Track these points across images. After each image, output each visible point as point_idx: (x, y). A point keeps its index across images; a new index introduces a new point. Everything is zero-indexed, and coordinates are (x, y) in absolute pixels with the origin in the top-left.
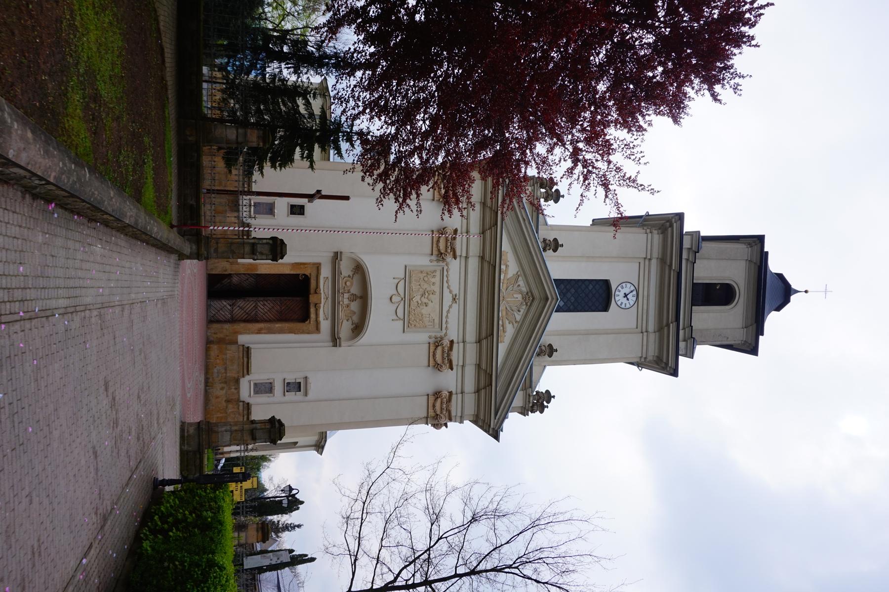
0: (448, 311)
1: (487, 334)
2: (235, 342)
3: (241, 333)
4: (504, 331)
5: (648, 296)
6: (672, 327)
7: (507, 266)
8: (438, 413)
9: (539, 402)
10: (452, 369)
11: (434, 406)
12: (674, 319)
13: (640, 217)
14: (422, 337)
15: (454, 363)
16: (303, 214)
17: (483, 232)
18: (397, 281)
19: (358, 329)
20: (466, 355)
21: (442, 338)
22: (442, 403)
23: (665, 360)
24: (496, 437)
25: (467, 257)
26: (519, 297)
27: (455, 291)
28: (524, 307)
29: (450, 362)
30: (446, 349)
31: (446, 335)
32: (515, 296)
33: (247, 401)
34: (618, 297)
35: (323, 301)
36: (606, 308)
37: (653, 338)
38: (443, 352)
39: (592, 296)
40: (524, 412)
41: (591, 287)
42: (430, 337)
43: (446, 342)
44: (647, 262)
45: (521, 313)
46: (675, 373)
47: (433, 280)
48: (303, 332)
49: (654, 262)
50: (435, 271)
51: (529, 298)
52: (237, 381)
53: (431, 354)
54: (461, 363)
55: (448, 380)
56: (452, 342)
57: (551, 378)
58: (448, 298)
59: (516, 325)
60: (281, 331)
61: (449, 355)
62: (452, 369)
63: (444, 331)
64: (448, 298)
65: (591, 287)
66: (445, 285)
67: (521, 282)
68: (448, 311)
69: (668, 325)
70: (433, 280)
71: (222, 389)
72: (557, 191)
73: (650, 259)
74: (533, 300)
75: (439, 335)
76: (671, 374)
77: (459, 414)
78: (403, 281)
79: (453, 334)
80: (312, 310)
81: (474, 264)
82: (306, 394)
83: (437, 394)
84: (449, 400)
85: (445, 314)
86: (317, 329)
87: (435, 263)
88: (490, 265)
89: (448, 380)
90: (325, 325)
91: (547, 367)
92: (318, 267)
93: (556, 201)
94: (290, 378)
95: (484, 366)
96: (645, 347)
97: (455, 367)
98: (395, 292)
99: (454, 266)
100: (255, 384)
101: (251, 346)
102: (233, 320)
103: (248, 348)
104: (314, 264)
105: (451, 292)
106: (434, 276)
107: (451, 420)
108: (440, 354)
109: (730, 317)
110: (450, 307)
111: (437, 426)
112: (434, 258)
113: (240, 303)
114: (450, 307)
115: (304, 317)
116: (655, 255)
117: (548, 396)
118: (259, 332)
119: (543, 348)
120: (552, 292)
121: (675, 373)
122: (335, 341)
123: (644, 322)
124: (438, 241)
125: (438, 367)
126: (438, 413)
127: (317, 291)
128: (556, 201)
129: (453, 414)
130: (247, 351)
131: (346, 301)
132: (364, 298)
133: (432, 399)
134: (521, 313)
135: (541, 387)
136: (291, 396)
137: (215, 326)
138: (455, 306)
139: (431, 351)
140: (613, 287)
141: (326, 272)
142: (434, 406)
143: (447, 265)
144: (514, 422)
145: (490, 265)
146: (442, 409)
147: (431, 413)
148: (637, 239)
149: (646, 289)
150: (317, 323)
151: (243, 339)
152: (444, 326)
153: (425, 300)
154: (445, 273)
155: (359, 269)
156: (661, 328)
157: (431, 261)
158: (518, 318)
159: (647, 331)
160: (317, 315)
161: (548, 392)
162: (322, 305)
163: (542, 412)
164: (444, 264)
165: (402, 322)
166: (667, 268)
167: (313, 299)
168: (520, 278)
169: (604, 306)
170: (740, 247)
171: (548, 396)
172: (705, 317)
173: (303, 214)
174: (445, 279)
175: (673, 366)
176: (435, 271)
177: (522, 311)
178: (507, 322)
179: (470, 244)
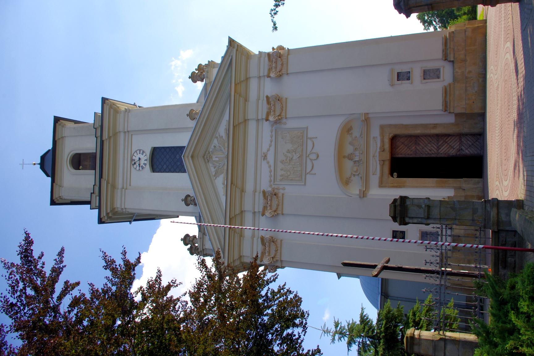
1: (238, 127)
2: (457, 115)
3: (452, 124)
5: (124, 160)
6: (105, 136)
8: (279, 58)
10: (267, 97)
11: (282, 65)
12: (105, 143)
13: (135, 220)
14: (291, 124)
16: (394, 231)
17: (242, 212)
18: (313, 172)
19: (347, 129)
20: (255, 108)
23: (112, 110)
24: (231, 42)
25: (255, 191)
26: (214, 159)
27: (264, 164)
28: (211, 150)
29: (268, 102)
31: (272, 126)
32: (217, 159)
33: (446, 62)
34: (145, 158)
35: (377, 154)
37: (120, 128)
38: (274, 111)
39: (165, 160)
40: (211, 64)
41: (165, 167)
43: (271, 118)
45: (213, 145)
46: (104, 100)
47: (283, 172)
48: (395, 126)
49: (120, 186)
50: (281, 180)
51: (207, 157)
52: (455, 79)
53: (284, 109)
58: (271, 157)
59: (217, 135)
60: (415, 126)
61: (270, 109)
62: (267, 97)
63: (273, 128)
64: (271, 157)
65: (165, 167)
66: (272, 168)
67: (213, 170)
69: (109, 137)
70: (283, 172)
71: (470, 72)
72: (186, 244)
73: (123, 188)
74: (204, 157)
76: (107, 99)
78: (308, 171)
79: (266, 127)
80: (387, 146)
81: (249, 186)
82: (392, 71)
83: (280, 76)
85: (273, 143)
86: (382, 127)
87: (281, 187)
88: (235, 185)
90: (375, 132)
92: (381, 185)
93: (187, 236)
94: (405, 85)
95: (242, 100)
96: (126, 119)
98: (314, 162)
99: (265, 185)
100: (438, 77)
101: (443, 113)
102: (460, 135)
103: (446, 111)
104: (385, 187)
105: (268, 163)
106: (281, 176)
107: (269, 54)
108: (276, 107)
109: (74, 145)
110: (268, 150)
111: (281, 48)
112: (281, 191)
113: (453, 152)
114: (268, 150)
115: (394, 139)
116: (119, 191)
117: (194, 78)
118: (435, 126)
120: (188, 163)
121: (104, 100)
122: (367, 120)
123: (126, 140)
124: (278, 205)
125: (279, 99)
127: (383, 162)
128: (187, 236)
129: (267, 58)
130: (446, 107)
131: (357, 153)
132: (341, 156)
133: (284, 71)
134: (213, 145)
135: (200, 85)
136: (404, 69)
137: (476, 130)
138: (265, 150)
139: (284, 111)
140: (148, 167)
141: (375, 179)
142: (282, 65)
143: (271, 186)
145: (235, 185)
146: (276, 63)
148: (130, 203)
149: (126, 165)
150: (382, 134)
151: (451, 119)
152: (274, 133)
153: (289, 155)
154: (272, 179)
155: (346, 182)
156: (116, 134)
157: (284, 189)
158: (215, 142)
160: (382, 141)
161: (195, 81)
162: (378, 150)
164: (273, 186)
165: (309, 136)
166: (110, 182)
167: (387, 156)
168: (214, 174)
169: (155, 151)
170: (67, 195)
171: (194, 78)
172: (88, 145)
173: (394, 231)
174: (272, 173)
175: (105, 106)
176: (281, 180)
177: (212, 147)
178: (224, 137)
179: (252, 202)
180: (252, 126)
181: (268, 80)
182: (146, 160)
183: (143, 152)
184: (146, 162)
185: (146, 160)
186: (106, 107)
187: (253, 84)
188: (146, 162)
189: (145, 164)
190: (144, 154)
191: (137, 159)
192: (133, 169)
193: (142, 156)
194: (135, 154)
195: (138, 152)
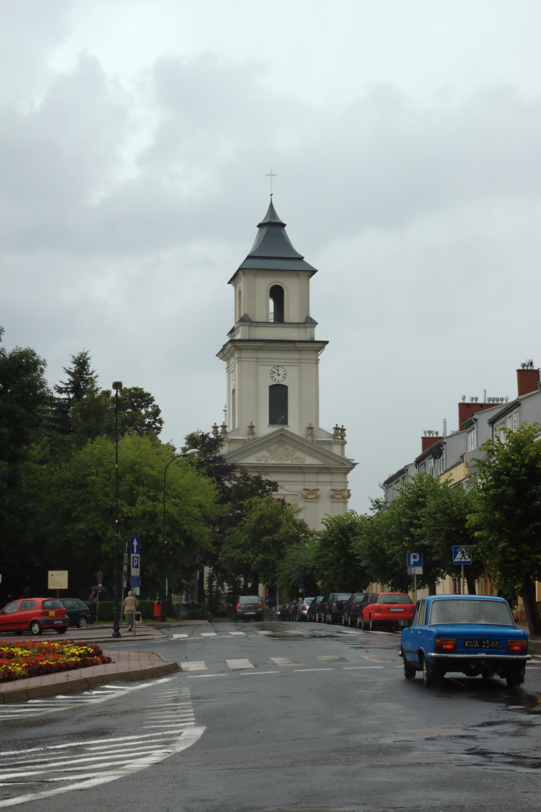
0: (288, 491)
1: (301, 469)
4: (299, 458)
6: (298, 345)
7: (264, 457)
9: (340, 433)
10: (318, 490)
11: (338, 499)
15: (315, 488)
20: (311, 481)
21: (302, 494)
22: (337, 494)
26: (280, 449)
28: (286, 446)
30: (308, 492)
31: (300, 492)
32: (280, 452)
34: (279, 380)
36: (285, 388)
39: (278, 396)
42: (302, 501)
44: (259, 360)
54: (316, 484)
55: (325, 490)
56: (305, 490)
57: (326, 425)
61: (311, 491)
67: (272, 448)
68: (288, 491)
73: (257, 358)
74: (281, 440)
75: (300, 496)
77: (343, 484)
79: (299, 488)
83: (332, 497)
84: (335, 490)
85: (289, 493)
89: (325, 490)
91: (320, 426)
96: (310, 361)
97: (318, 487)
110: (285, 490)
111: (349, 496)
114: (285, 490)
117: (336, 429)
119: (309, 433)
126: (341, 496)
129: (343, 488)
133: (335, 500)
142: (338, 499)
144: (349, 453)
146: (340, 494)
147: (342, 500)
156: (299, 350)
158: (291, 449)
159: (300, 360)
163: (345, 430)
168: (270, 449)
169: (285, 388)
171: (336, 429)
180: (299, 477)
181: (330, 488)
182: (278, 381)
183: (284, 378)
184: (277, 381)
185: (278, 381)
186: (320, 345)
187: (327, 478)
188: (277, 381)
189: (275, 380)
190: (283, 379)
191: (280, 372)
192: (271, 367)
193: (281, 376)
194: (283, 370)
195: (284, 373)
